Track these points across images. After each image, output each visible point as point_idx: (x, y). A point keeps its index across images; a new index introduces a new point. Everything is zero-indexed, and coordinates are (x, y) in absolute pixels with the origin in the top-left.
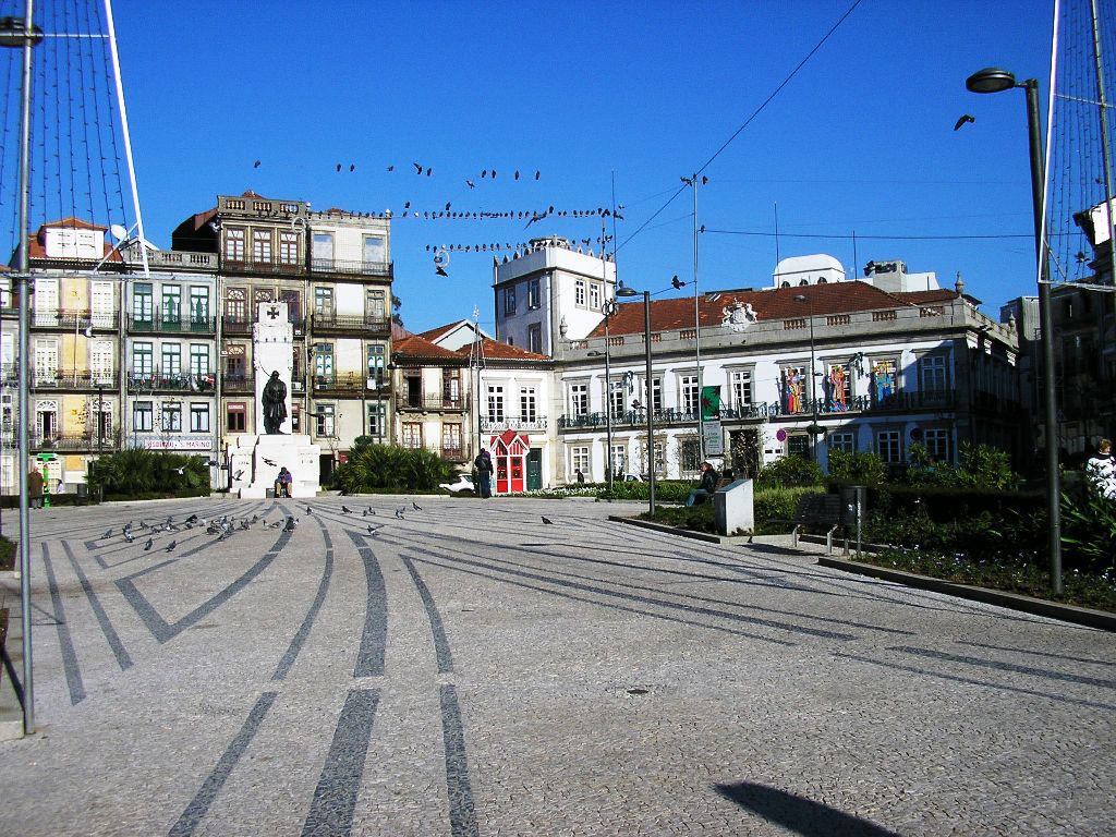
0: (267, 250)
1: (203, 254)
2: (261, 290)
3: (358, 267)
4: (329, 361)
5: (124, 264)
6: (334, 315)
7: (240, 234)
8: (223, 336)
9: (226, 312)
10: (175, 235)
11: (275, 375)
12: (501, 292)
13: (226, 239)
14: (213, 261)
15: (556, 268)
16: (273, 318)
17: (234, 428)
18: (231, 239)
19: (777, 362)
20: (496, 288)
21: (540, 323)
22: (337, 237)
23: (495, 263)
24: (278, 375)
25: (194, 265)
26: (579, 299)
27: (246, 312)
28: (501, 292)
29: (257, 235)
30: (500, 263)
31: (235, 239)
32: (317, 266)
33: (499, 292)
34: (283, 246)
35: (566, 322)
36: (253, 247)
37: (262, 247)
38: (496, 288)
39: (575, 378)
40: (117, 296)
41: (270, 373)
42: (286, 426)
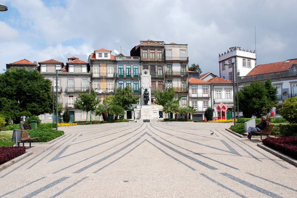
3: (178, 59)
4: (171, 85)
5: (116, 60)
6: (172, 72)
10: (131, 52)
11: (146, 90)
12: (221, 64)
16: (146, 74)
19: (289, 82)
20: (220, 62)
22: (173, 50)
23: (220, 56)
24: (147, 90)
25: (134, 60)
26: (244, 65)
28: (221, 64)
30: (221, 55)
32: (167, 59)
33: (220, 64)
35: (240, 71)
38: (220, 62)
40: (114, 69)
41: (145, 89)
42: (149, 102)
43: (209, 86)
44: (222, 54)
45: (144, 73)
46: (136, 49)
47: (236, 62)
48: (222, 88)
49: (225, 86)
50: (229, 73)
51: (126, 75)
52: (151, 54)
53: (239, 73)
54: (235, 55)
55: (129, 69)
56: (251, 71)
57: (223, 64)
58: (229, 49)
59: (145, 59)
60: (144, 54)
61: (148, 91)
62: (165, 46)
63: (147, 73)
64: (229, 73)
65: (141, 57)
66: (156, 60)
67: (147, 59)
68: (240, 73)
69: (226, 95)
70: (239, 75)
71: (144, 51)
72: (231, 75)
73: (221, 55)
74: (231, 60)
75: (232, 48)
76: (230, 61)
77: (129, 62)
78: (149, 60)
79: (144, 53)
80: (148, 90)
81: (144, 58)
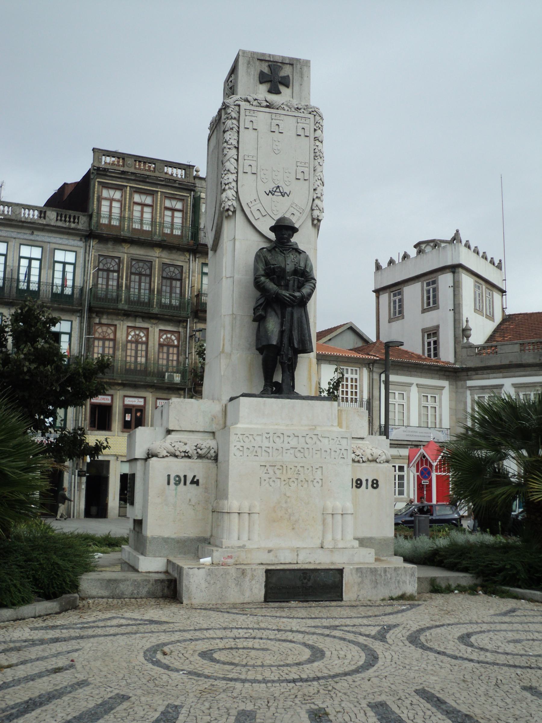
0: (147, 216)
1: (72, 213)
2: (138, 261)
7: (117, 195)
8: (91, 310)
9: (96, 285)
12: (385, 297)
13: (100, 199)
14: (82, 223)
15: (460, 266)
16: (274, 90)
17: (94, 427)
18: (106, 199)
21: (438, 327)
23: (378, 267)
25: (59, 224)
27: (119, 286)
29: (137, 198)
31: (111, 200)
34: (133, 277)
35: (471, 325)
36: (131, 211)
37: (142, 212)
38: (378, 292)
39: (483, 388)
43: (365, 371)
44: (391, 262)
45: (263, 78)
46: (68, 191)
47: (459, 287)
48: (410, 385)
49: (421, 377)
50: (424, 331)
51: (14, 290)
52: (138, 208)
53: (468, 332)
54: (455, 262)
55: (33, 262)
56: (495, 331)
57: (392, 298)
58: (415, 246)
59: (109, 226)
60: (105, 204)
61: (298, 251)
62: (197, 182)
63: (286, 82)
64: (424, 331)
65: (90, 217)
66: (156, 238)
67: (120, 228)
68: (472, 332)
69: (423, 411)
70: (468, 337)
71: (105, 193)
72: (432, 340)
73: (384, 264)
74: (434, 282)
75: (427, 242)
76: (428, 284)
77: (36, 233)
78: (125, 234)
79: (106, 199)
80: (295, 239)
81: (104, 221)
